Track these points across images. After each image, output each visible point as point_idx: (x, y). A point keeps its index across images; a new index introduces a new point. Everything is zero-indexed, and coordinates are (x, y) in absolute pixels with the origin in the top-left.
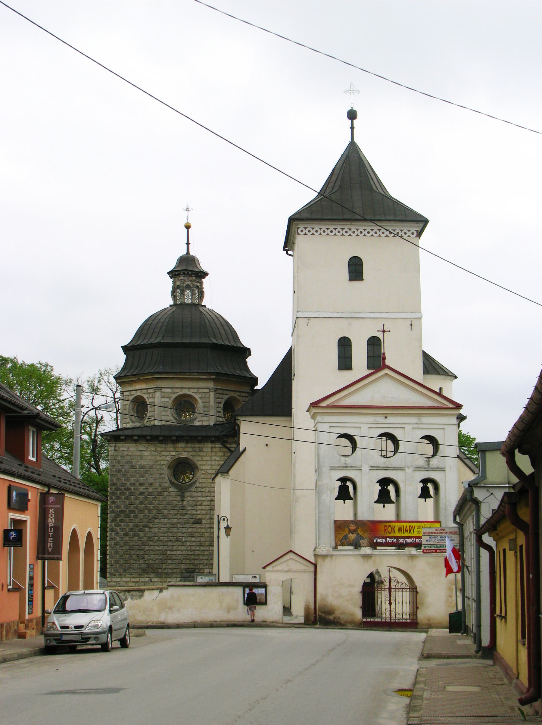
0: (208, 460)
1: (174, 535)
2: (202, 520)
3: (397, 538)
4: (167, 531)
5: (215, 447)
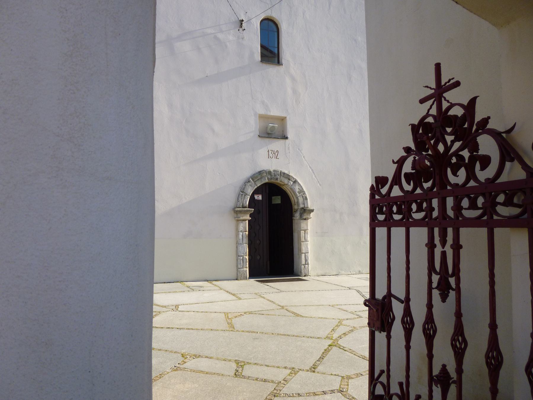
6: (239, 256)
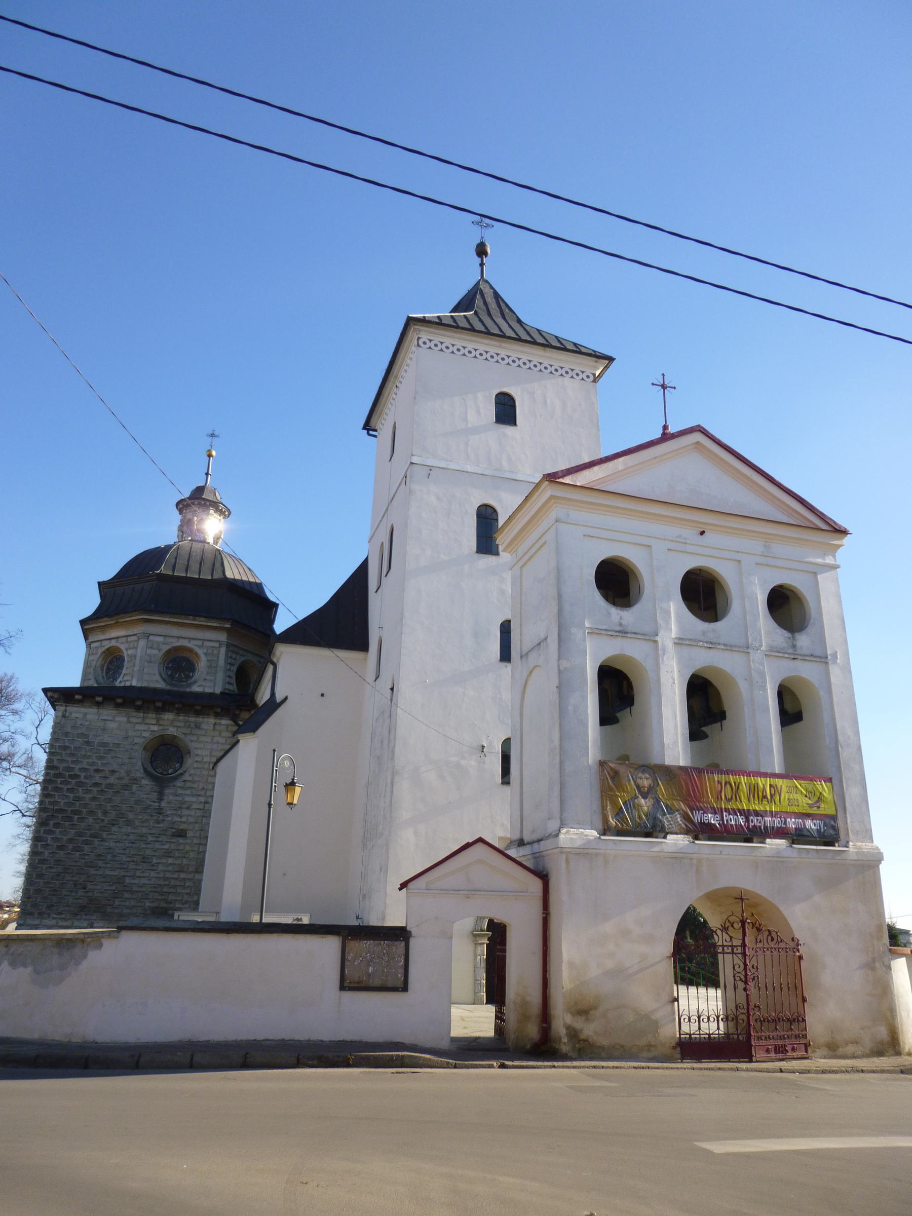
0: (207, 742)
1: (140, 853)
2: (188, 832)
3: (746, 814)
4: (130, 845)
5: (220, 724)
6: (476, 980)
